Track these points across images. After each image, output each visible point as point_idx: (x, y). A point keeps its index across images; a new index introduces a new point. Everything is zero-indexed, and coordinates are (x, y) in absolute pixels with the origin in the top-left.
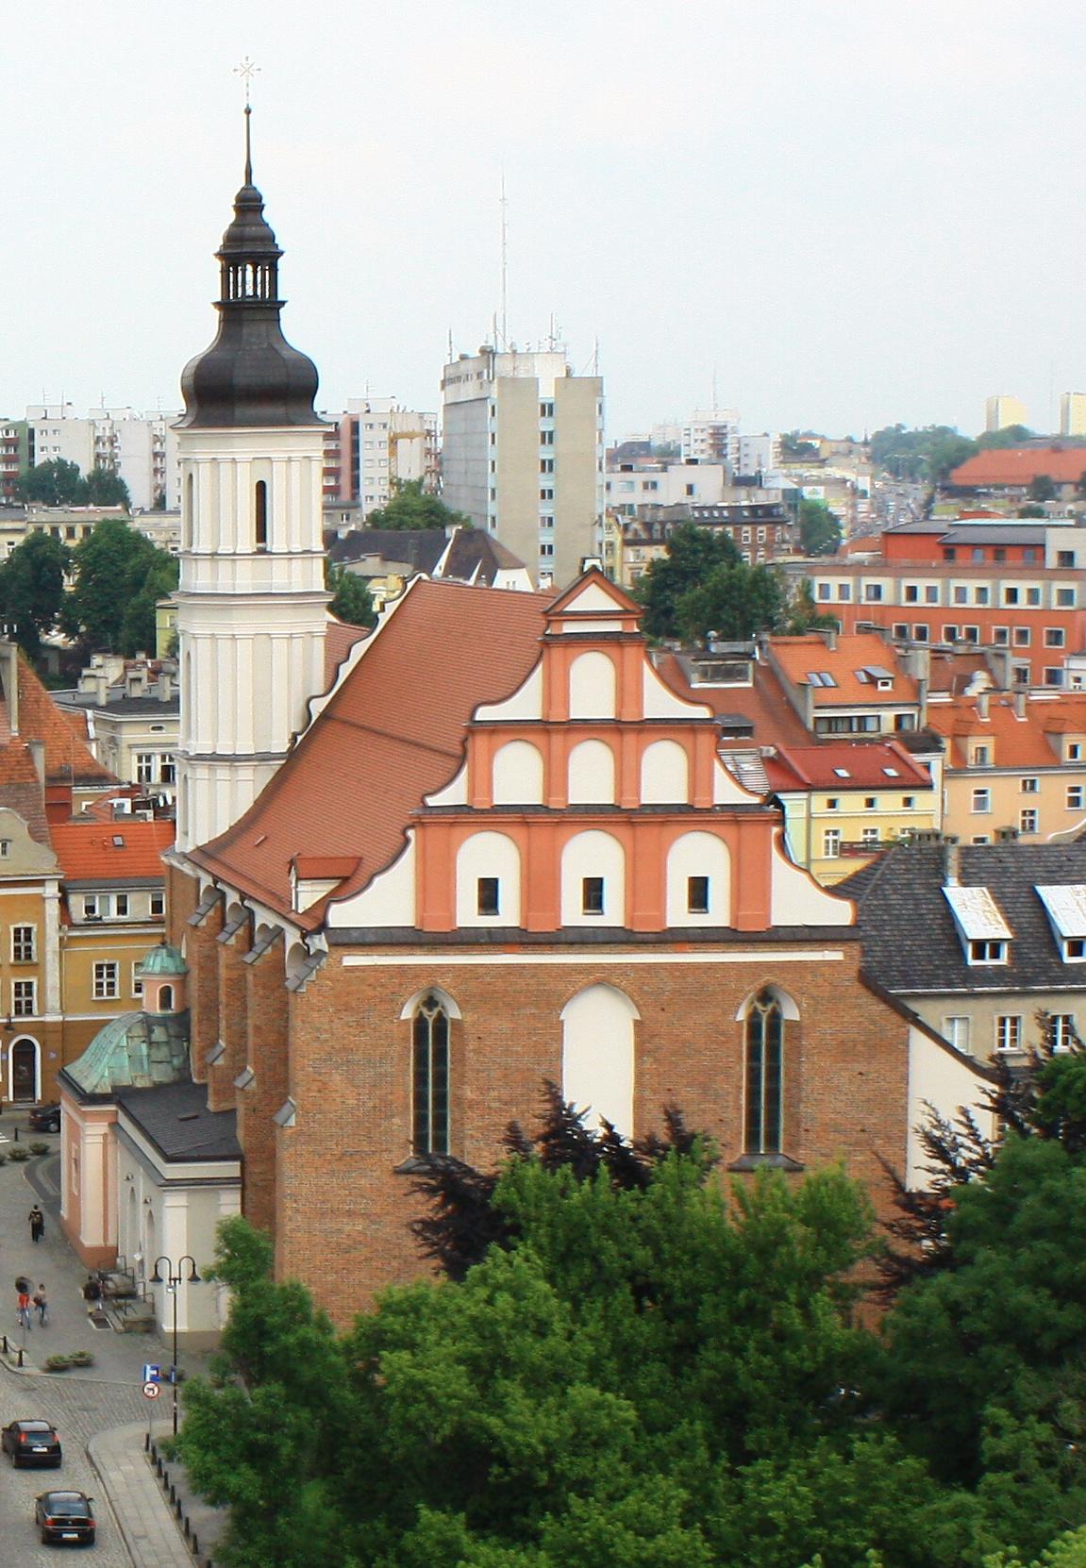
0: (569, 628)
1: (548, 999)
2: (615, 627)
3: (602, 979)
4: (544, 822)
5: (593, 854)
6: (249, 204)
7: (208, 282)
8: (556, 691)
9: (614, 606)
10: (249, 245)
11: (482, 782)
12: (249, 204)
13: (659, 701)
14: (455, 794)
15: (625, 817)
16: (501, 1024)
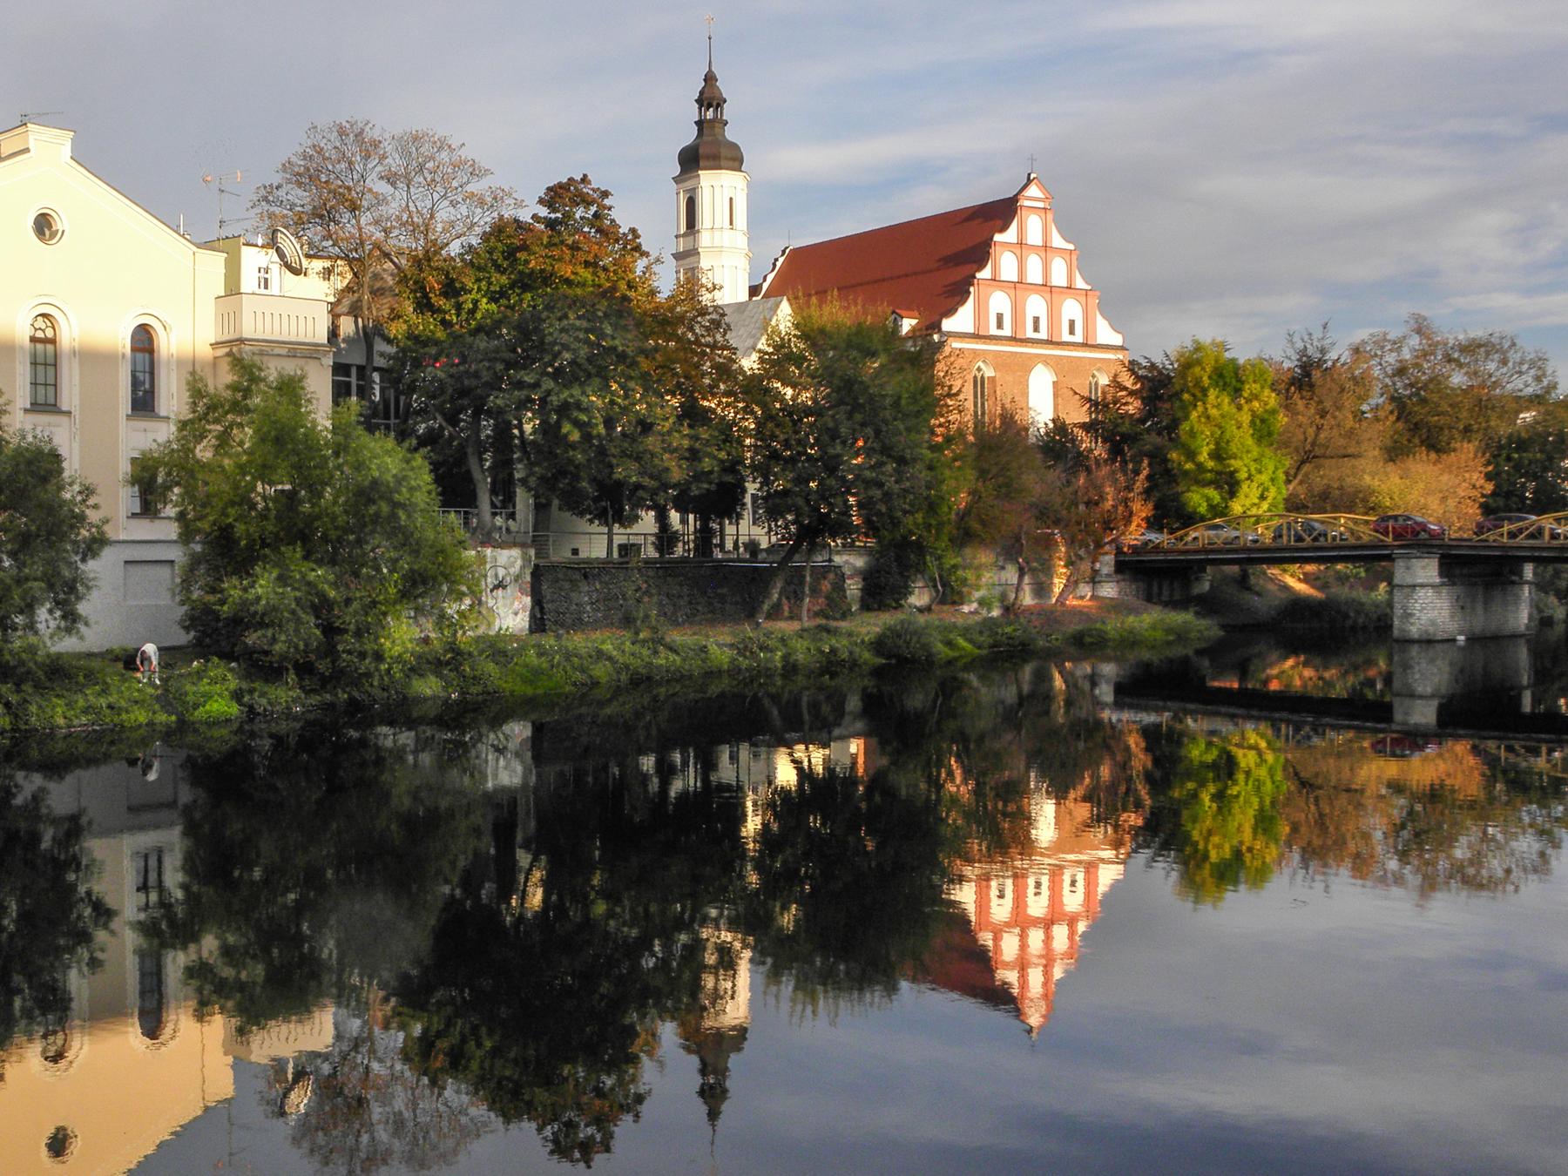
0: (1027, 203)
1: (1026, 365)
2: (1041, 205)
3: (1046, 360)
4: (1019, 287)
5: (1036, 306)
6: (710, 78)
7: (693, 112)
8: (1021, 231)
9: (1041, 196)
10: (710, 98)
11: (995, 270)
12: (710, 78)
13: (1057, 241)
14: (985, 274)
15: (1046, 287)
16: (1010, 378)
